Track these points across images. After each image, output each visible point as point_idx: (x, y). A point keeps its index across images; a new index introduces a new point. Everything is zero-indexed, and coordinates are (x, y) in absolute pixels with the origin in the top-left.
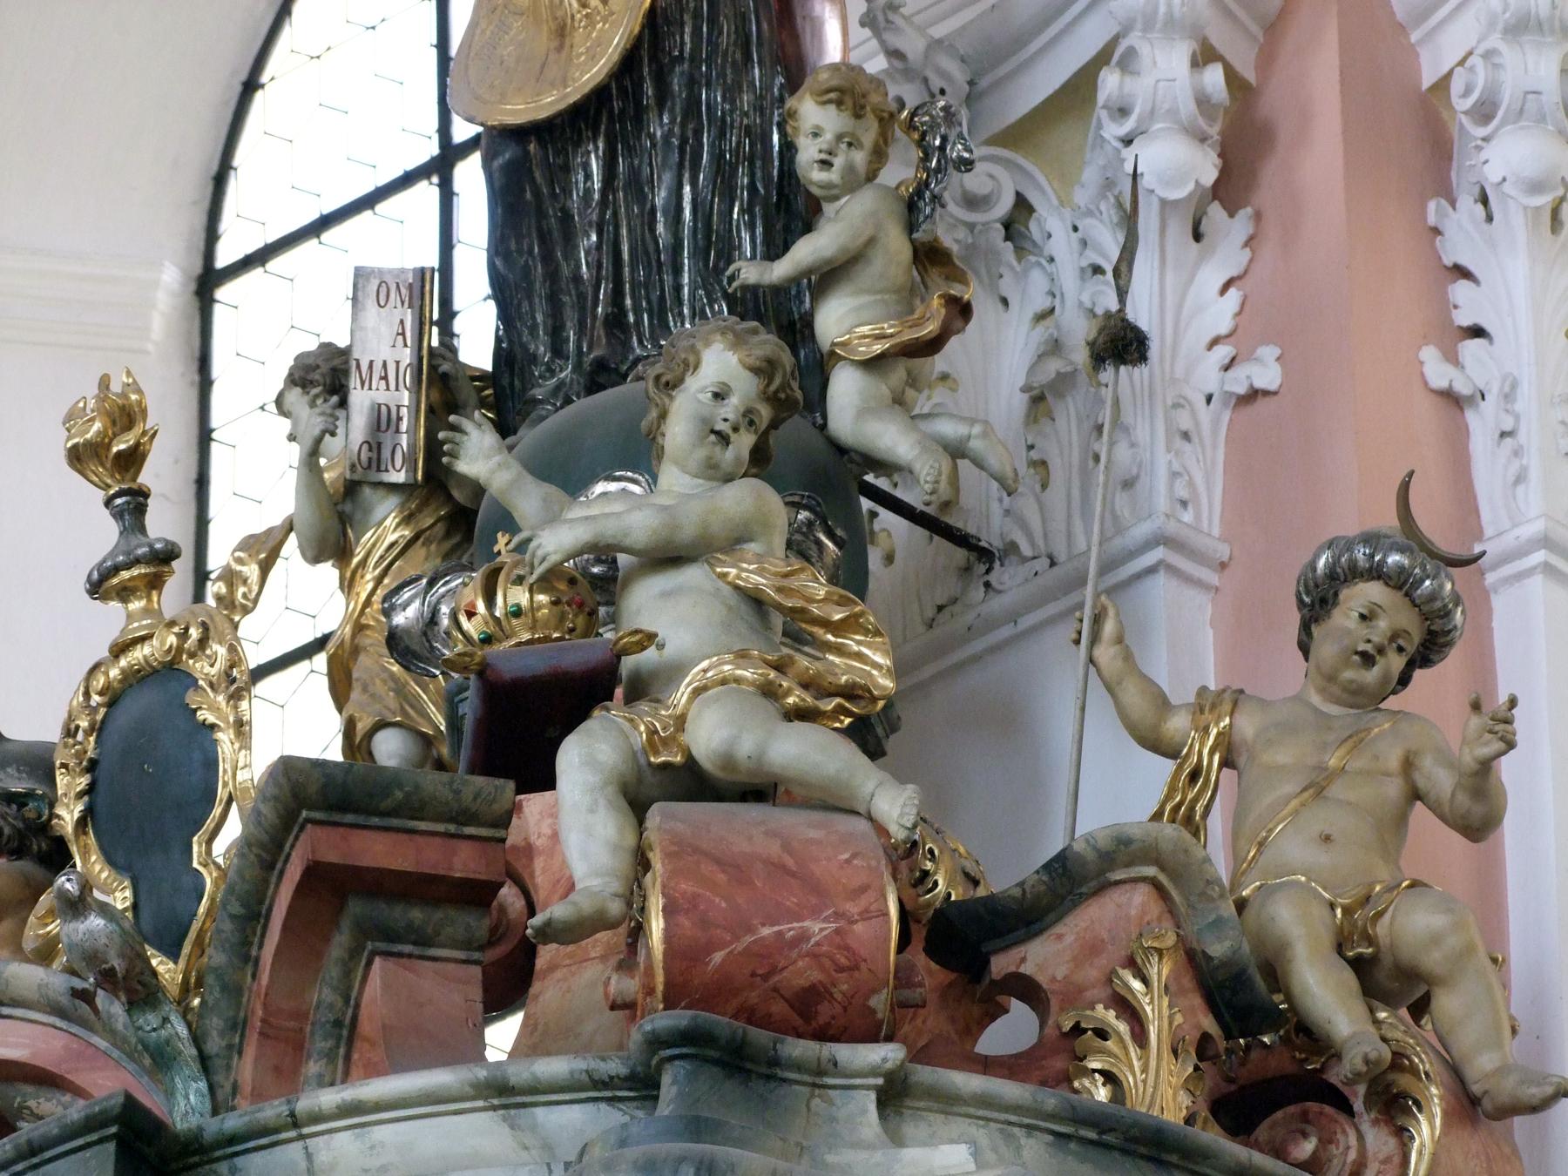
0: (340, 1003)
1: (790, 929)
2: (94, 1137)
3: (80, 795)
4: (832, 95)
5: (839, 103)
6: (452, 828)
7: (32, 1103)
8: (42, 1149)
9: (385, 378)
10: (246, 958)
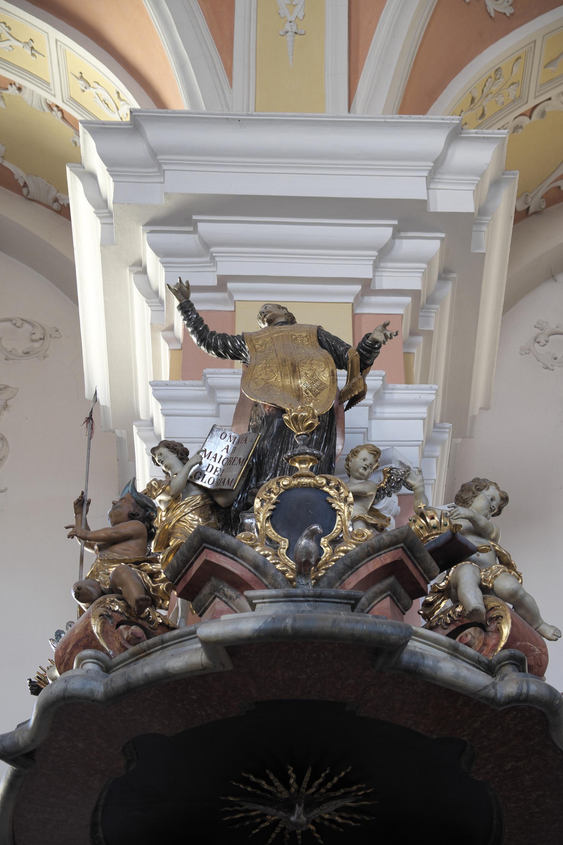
0: (367, 605)
1: (533, 647)
2: (345, 601)
3: (270, 510)
4: (375, 453)
5: (375, 456)
6: (423, 572)
7: (226, 589)
8: (323, 597)
9: (215, 458)
10: (340, 579)
